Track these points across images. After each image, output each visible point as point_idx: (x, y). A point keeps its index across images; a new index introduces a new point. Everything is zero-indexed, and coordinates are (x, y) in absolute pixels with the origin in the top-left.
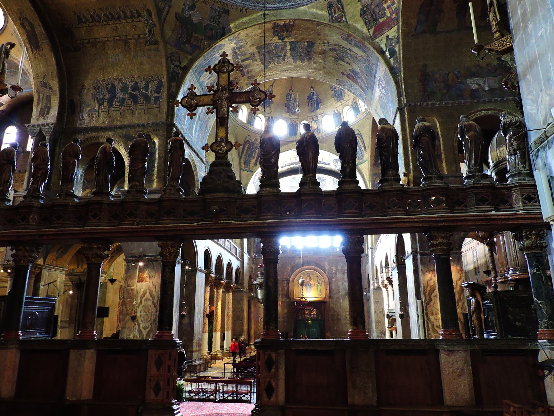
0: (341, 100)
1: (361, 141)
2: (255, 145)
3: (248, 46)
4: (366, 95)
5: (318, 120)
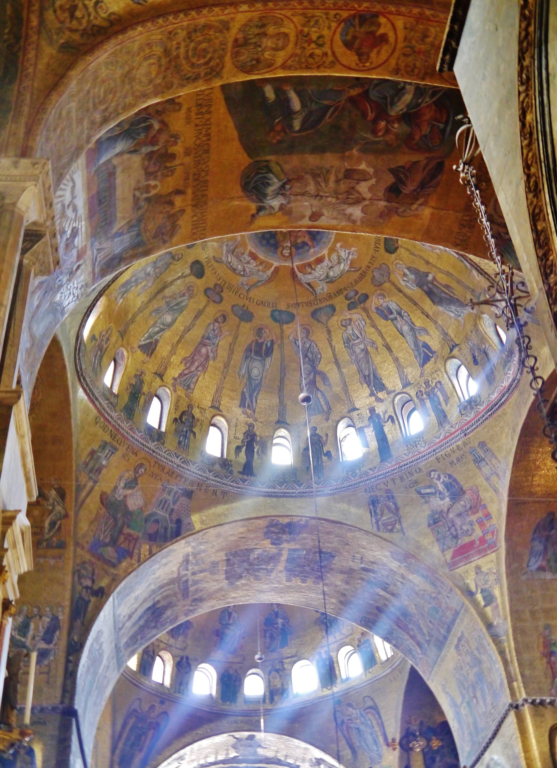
1: (378, 723)
2: (149, 720)
3: (213, 550)
4: (424, 654)
5: (284, 669)
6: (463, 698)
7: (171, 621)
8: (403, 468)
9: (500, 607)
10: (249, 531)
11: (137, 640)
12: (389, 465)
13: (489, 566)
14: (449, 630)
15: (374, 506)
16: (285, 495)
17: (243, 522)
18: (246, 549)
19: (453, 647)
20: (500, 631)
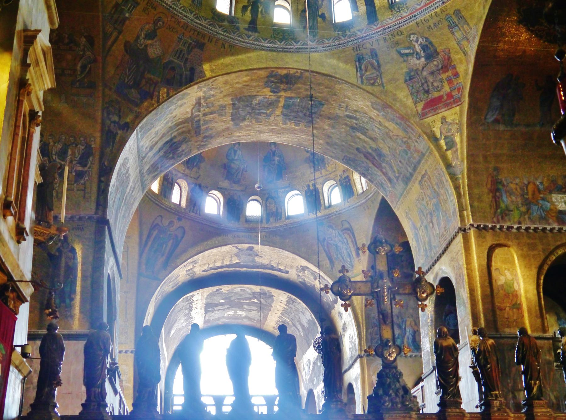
0: (321, 169)
1: (352, 241)
2: (169, 233)
3: (222, 95)
4: (393, 187)
6: (422, 223)
7: (185, 153)
8: (387, 31)
9: (459, 151)
10: (252, 80)
11: (158, 168)
12: (375, 27)
13: (453, 117)
14: (415, 169)
15: (359, 63)
16: (283, 50)
17: (247, 72)
18: (249, 96)
19: (417, 182)
20: (457, 171)
